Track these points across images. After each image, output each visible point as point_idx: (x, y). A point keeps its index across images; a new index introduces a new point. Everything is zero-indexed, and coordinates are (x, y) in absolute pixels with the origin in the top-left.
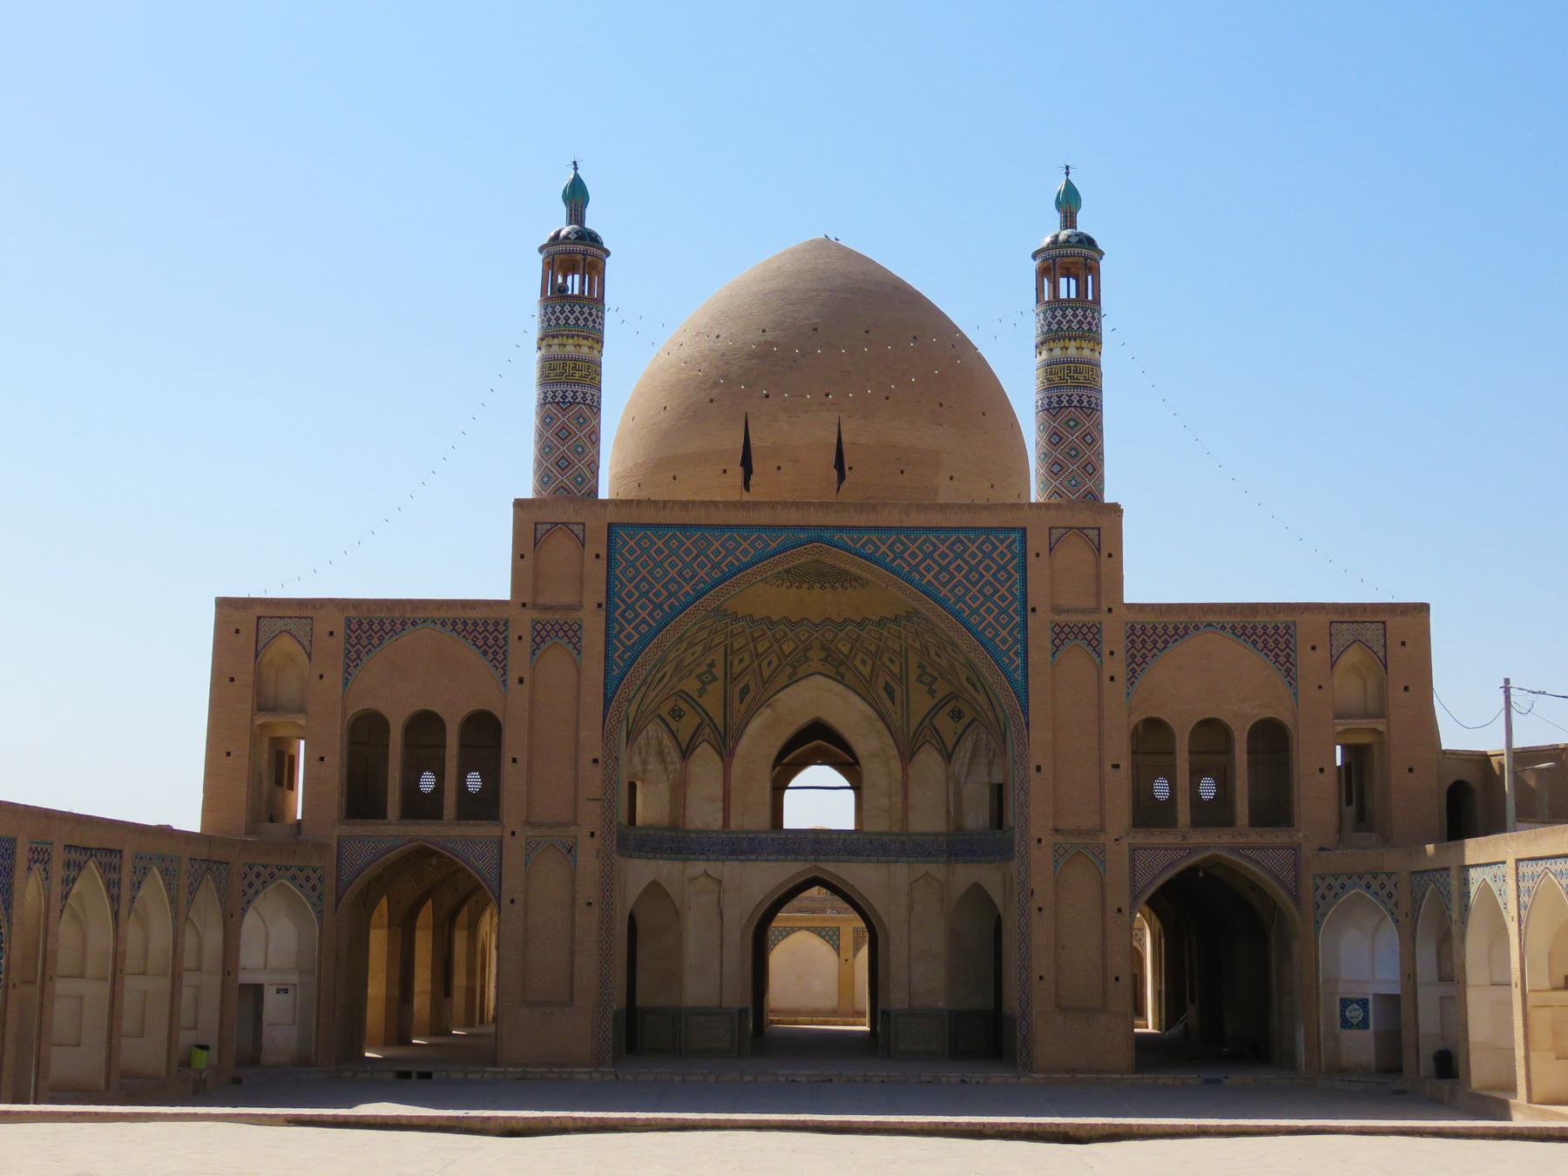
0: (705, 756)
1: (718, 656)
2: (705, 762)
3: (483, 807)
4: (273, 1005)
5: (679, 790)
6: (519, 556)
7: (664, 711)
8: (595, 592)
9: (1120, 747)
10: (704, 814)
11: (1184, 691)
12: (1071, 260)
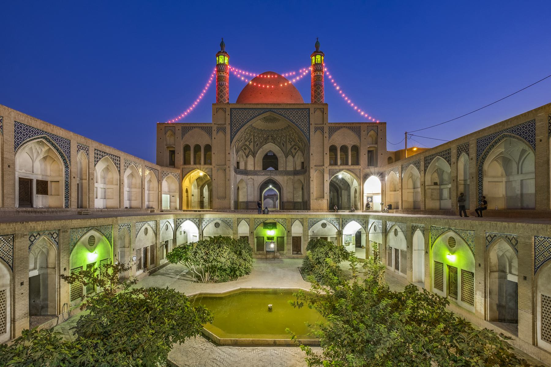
0: (251, 157)
1: (252, 137)
2: (250, 159)
7: (243, 148)
8: (228, 121)
9: (327, 150)
10: (250, 167)
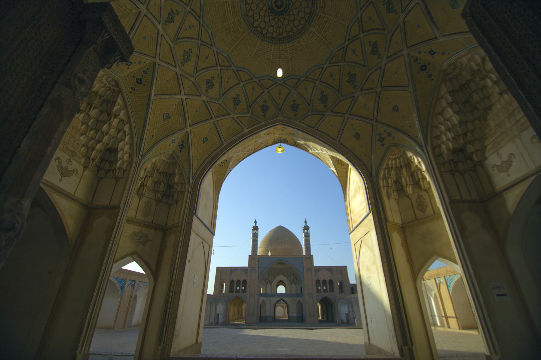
0: (269, 284)
3: (244, 291)
4: (220, 316)
5: (266, 289)
6: (249, 261)
9: (314, 283)
10: (269, 292)
11: (321, 277)
12: (306, 228)
